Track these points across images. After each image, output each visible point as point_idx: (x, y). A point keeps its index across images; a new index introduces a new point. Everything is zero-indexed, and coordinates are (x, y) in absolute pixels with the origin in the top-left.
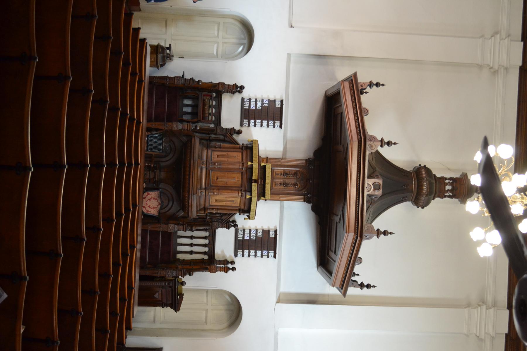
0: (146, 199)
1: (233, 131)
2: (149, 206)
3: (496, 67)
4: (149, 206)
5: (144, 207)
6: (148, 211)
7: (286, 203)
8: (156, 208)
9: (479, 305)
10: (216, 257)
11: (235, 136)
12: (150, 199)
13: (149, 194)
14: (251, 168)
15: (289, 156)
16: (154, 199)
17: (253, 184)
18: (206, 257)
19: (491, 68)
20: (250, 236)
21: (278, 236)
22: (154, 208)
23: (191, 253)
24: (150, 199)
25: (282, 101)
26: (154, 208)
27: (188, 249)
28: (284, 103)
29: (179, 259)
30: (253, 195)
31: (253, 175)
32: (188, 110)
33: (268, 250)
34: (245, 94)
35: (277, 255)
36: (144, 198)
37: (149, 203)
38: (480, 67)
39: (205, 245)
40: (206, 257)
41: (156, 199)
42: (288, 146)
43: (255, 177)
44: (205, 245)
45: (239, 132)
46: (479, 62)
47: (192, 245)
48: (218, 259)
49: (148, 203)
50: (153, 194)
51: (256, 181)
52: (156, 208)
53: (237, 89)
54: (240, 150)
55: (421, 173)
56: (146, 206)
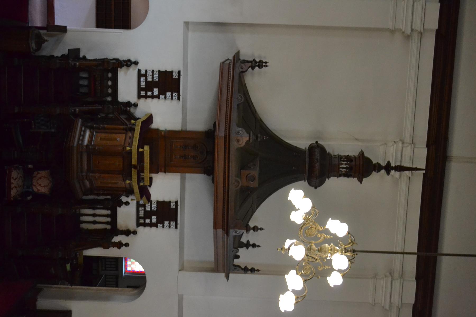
1: (128, 104)
2: (40, 185)
3: (408, 32)
5: (35, 186)
6: (39, 190)
7: (188, 175)
8: (46, 186)
9: (386, 276)
10: (119, 227)
11: (132, 110)
12: (40, 178)
13: (38, 173)
14: (130, 153)
15: (191, 127)
16: (44, 177)
17: (133, 169)
18: (109, 227)
19: (403, 32)
20: (151, 208)
21: (179, 207)
22: (44, 186)
23: (94, 222)
24: (40, 178)
25: (179, 72)
26: (44, 186)
27: (91, 219)
28: (181, 73)
29: (83, 229)
30: (133, 180)
31: (133, 160)
32: (85, 82)
33: (170, 221)
34: (140, 66)
35: (179, 226)
37: (40, 182)
38: (392, 32)
39: (107, 216)
40: (109, 227)
42: (189, 117)
43: (134, 161)
44: (107, 216)
45: (136, 105)
46: (390, 26)
47: (94, 215)
48: (121, 229)
50: (43, 173)
51: (135, 167)
53: (128, 63)
54: (124, 131)
55: (317, 150)
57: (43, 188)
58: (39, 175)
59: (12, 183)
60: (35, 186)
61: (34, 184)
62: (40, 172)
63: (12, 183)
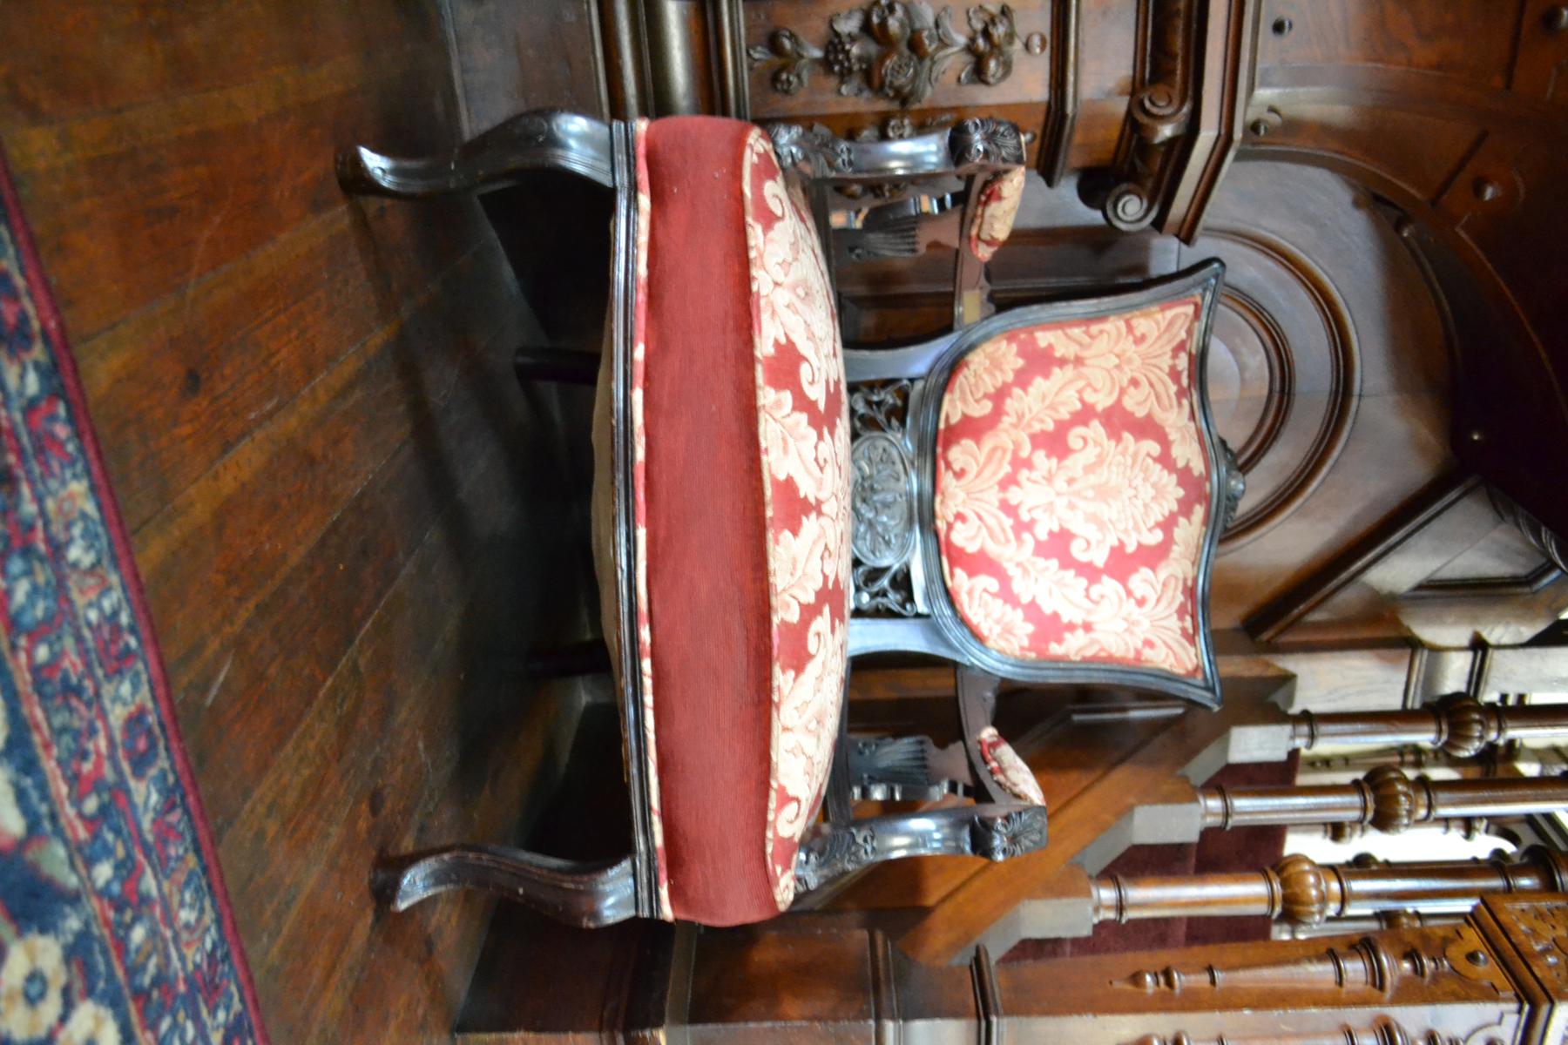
0: (1005, 436)
2: (1058, 546)
4: (1058, 546)
5: (979, 564)
6: (1049, 626)
8: (1152, 556)
13: (1039, 362)
16: (1118, 422)
22: (1122, 564)
24: (1055, 442)
26: (1122, 564)
36: (972, 428)
37: (1046, 496)
41: (1147, 428)
49: (1030, 495)
52: (1152, 556)
56: (1010, 554)
57: (1109, 585)
58: (1039, 384)
59: (797, 508)
60: (979, 564)
61: (962, 537)
62: (1044, 338)
63: (797, 508)
